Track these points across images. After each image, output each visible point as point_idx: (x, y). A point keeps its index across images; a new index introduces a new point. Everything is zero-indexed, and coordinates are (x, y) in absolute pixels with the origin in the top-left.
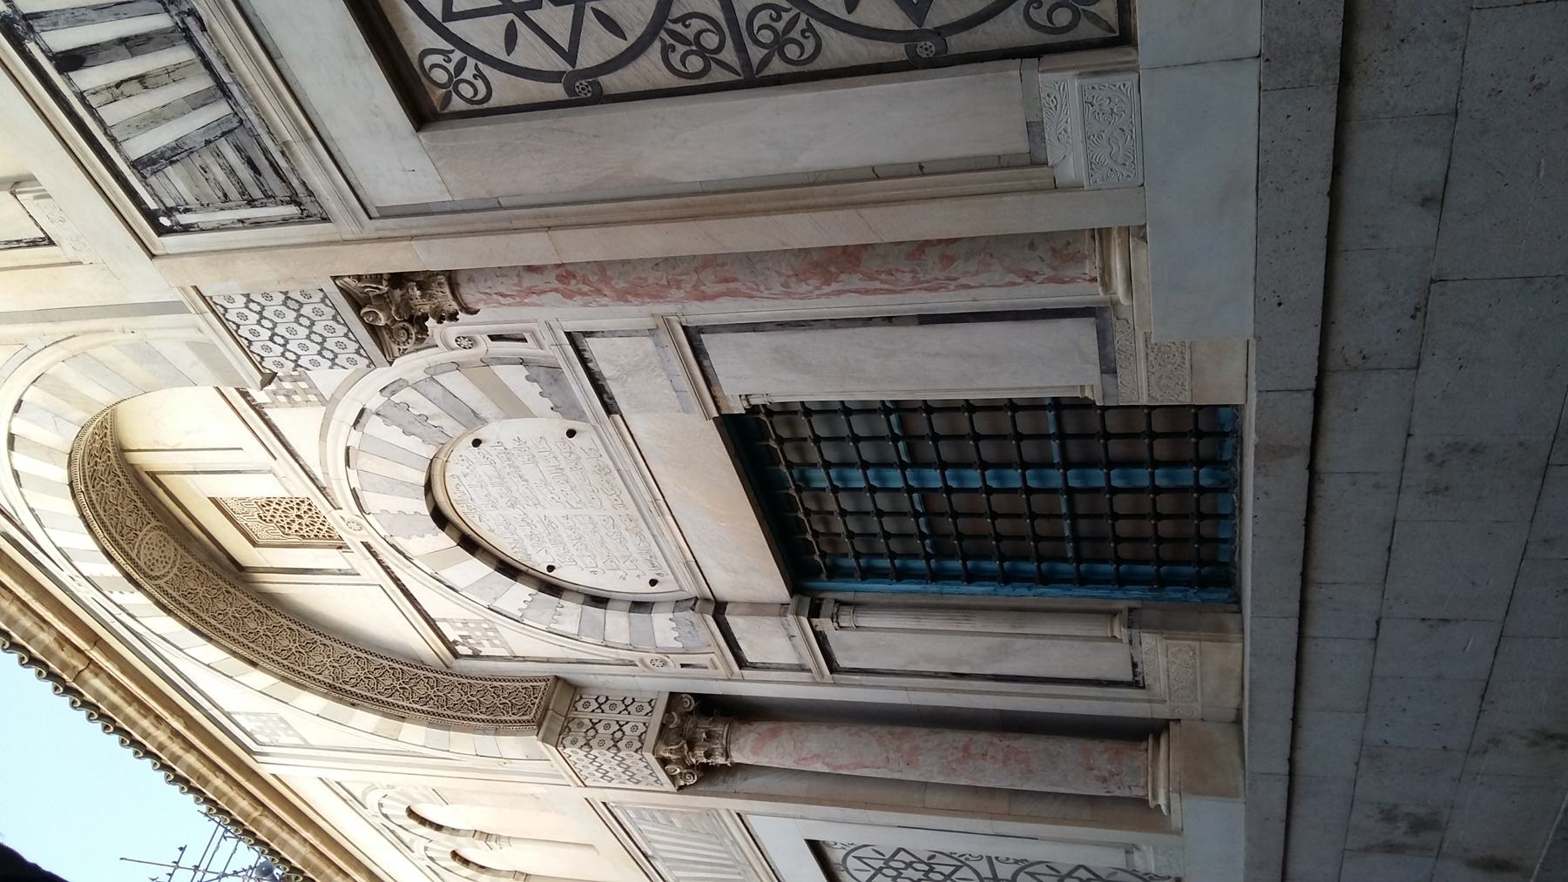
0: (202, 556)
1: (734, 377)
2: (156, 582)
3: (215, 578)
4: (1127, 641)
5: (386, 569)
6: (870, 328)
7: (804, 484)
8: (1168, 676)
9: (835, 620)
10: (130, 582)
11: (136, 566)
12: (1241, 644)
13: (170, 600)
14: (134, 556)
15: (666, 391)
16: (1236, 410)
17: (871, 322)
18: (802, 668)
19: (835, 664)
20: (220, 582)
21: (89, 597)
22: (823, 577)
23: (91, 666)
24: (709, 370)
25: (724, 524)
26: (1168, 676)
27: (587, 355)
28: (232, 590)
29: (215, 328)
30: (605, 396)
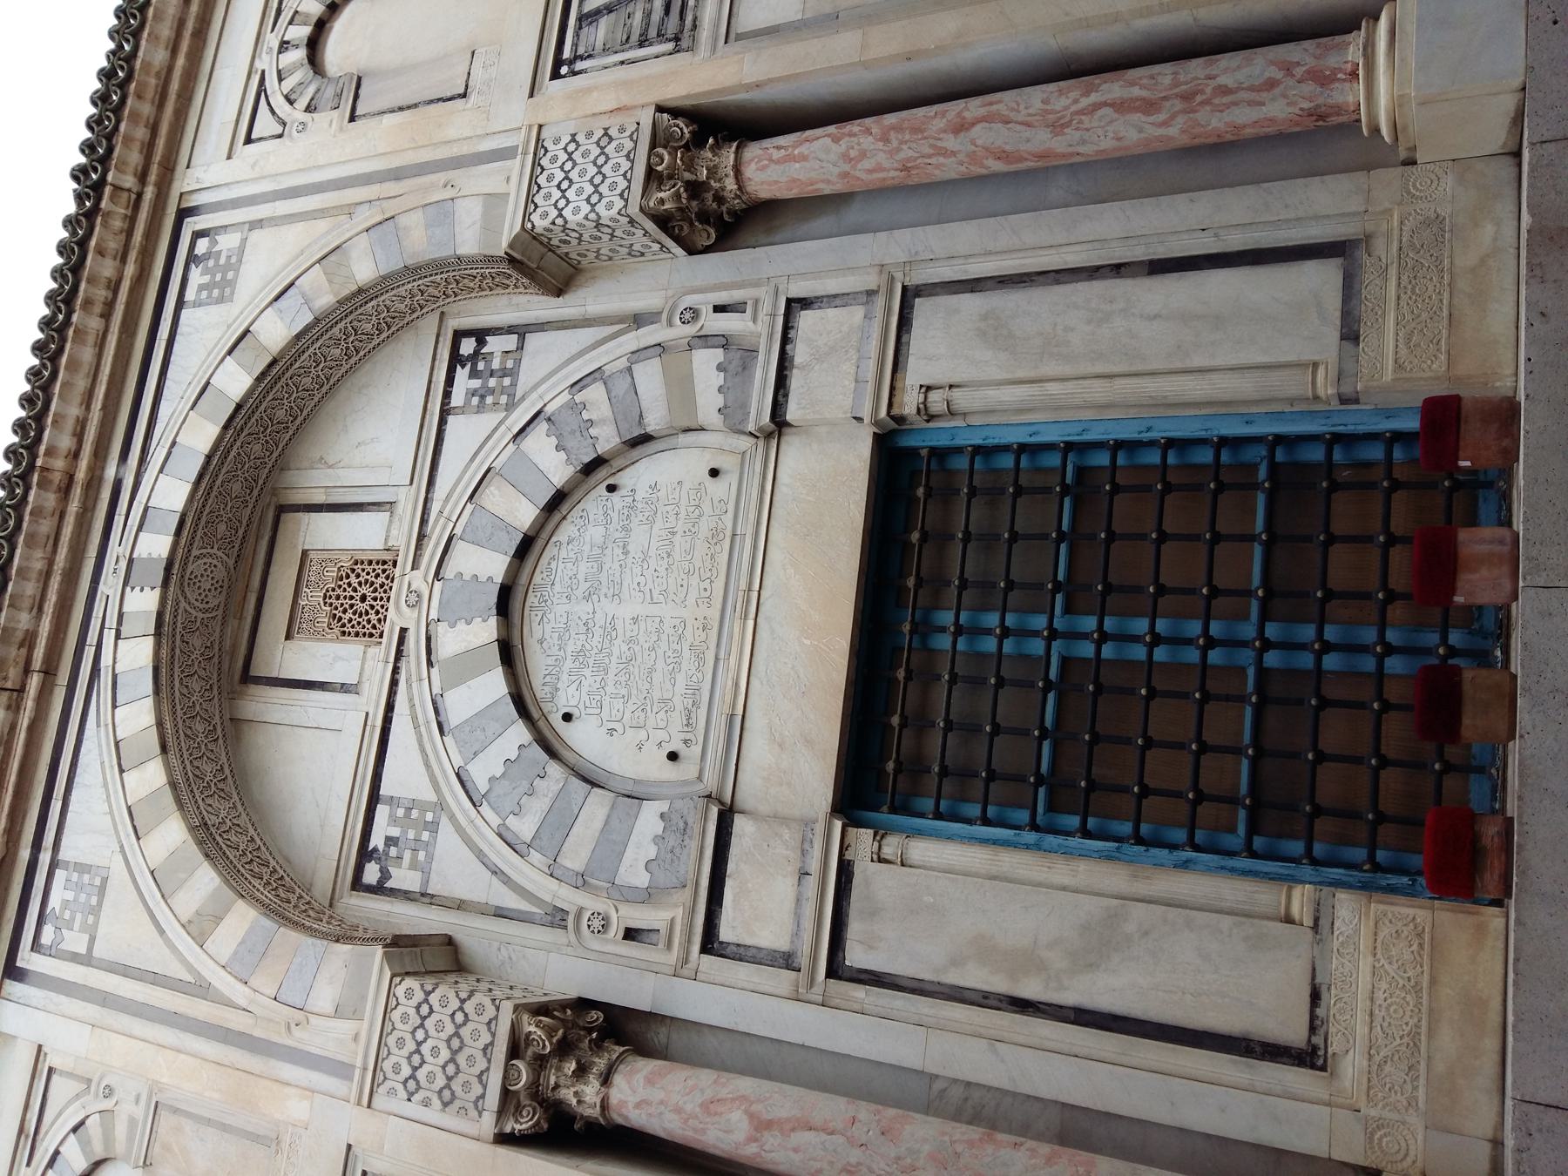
0: (228, 643)
1: (925, 358)
2: (182, 599)
3: (216, 668)
4: (1311, 925)
5: (390, 707)
6: (1094, 282)
7: (925, 629)
8: (1371, 1014)
9: (878, 838)
10: (165, 569)
11: (185, 562)
12: (1503, 920)
13: (171, 623)
14: (195, 552)
15: (847, 383)
16: (1506, 414)
17: (1098, 274)
18: (787, 961)
19: (841, 955)
20: (215, 675)
21: (110, 592)
22: (885, 808)
23: (15, 694)
24: (904, 348)
25: (807, 642)
26: (1371, 1014)
27: (792, 334)
28: (215, 692)
29: (525, 163)
30: (781, 392)
